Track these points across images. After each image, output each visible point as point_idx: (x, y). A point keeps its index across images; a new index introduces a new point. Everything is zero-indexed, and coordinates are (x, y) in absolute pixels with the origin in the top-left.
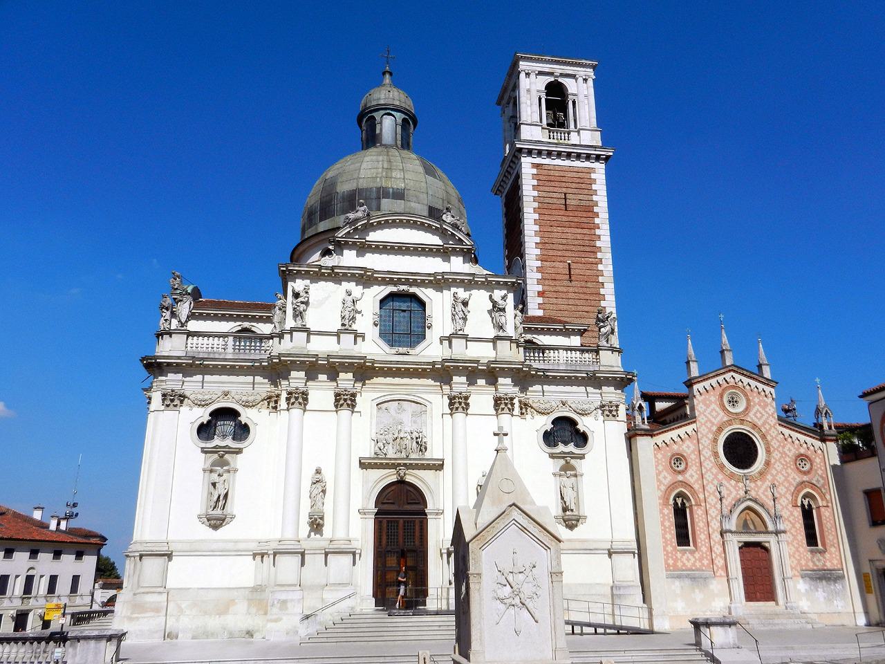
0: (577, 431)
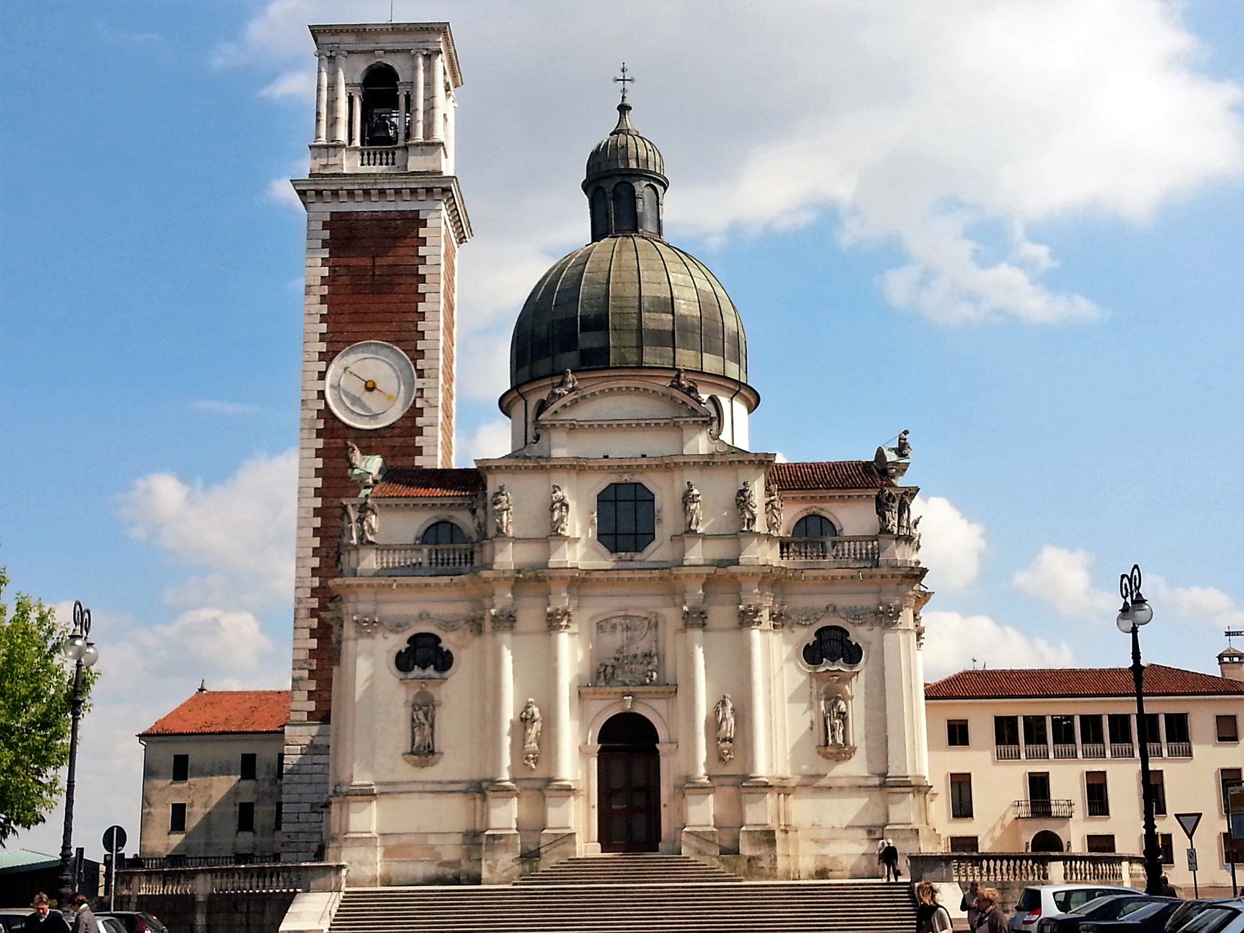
0: (850, 642)
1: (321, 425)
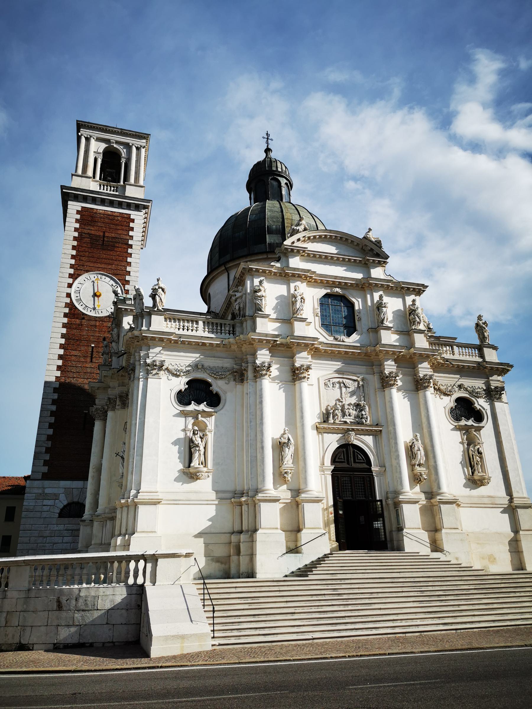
1: (67, 310)
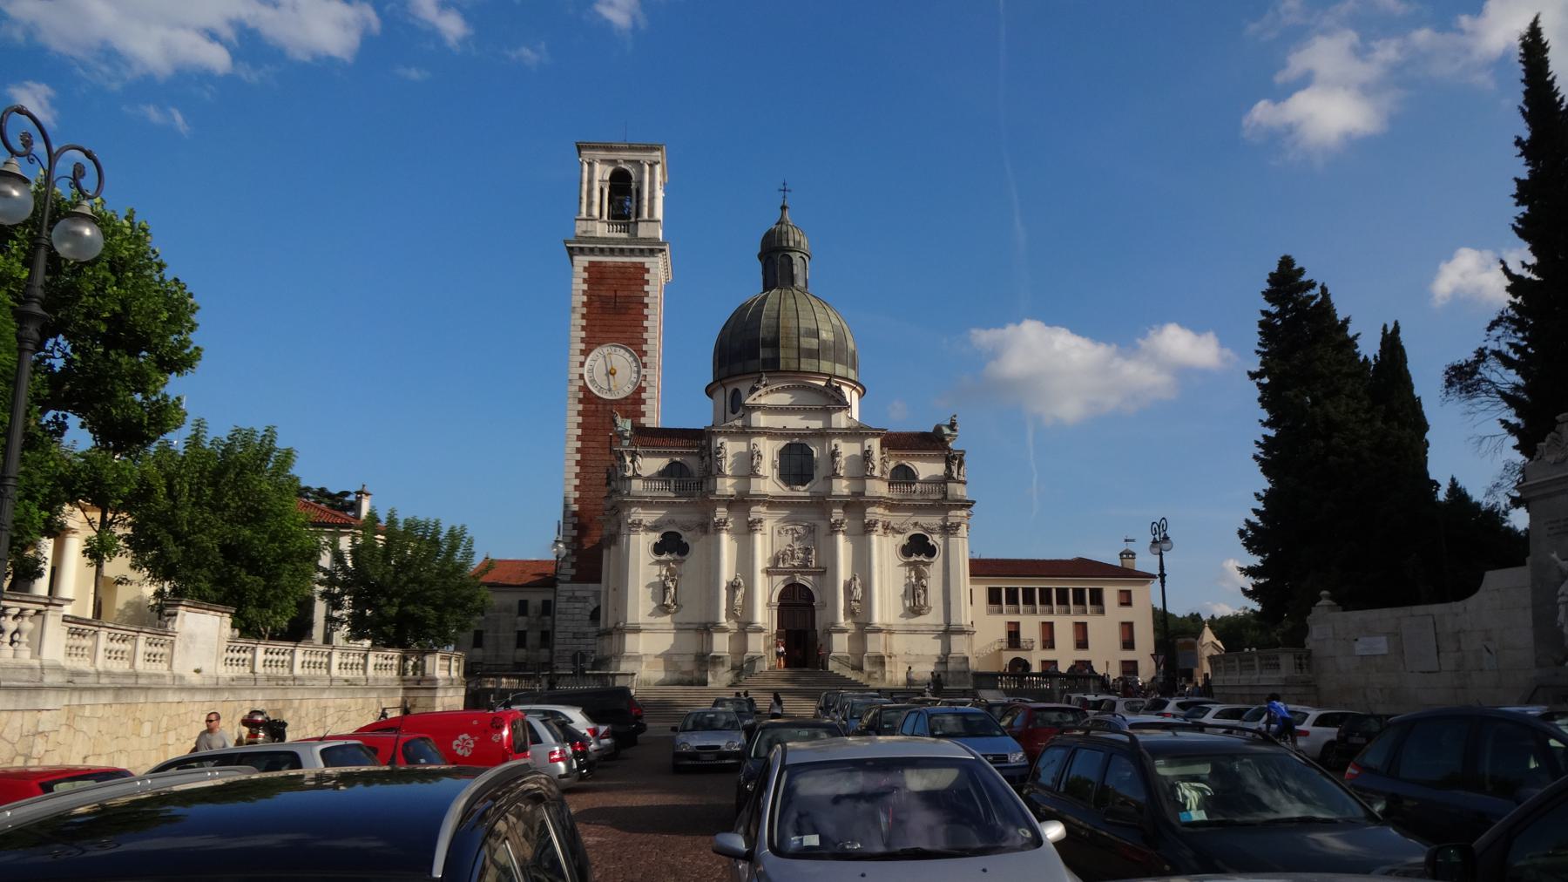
0: (929, 544)
